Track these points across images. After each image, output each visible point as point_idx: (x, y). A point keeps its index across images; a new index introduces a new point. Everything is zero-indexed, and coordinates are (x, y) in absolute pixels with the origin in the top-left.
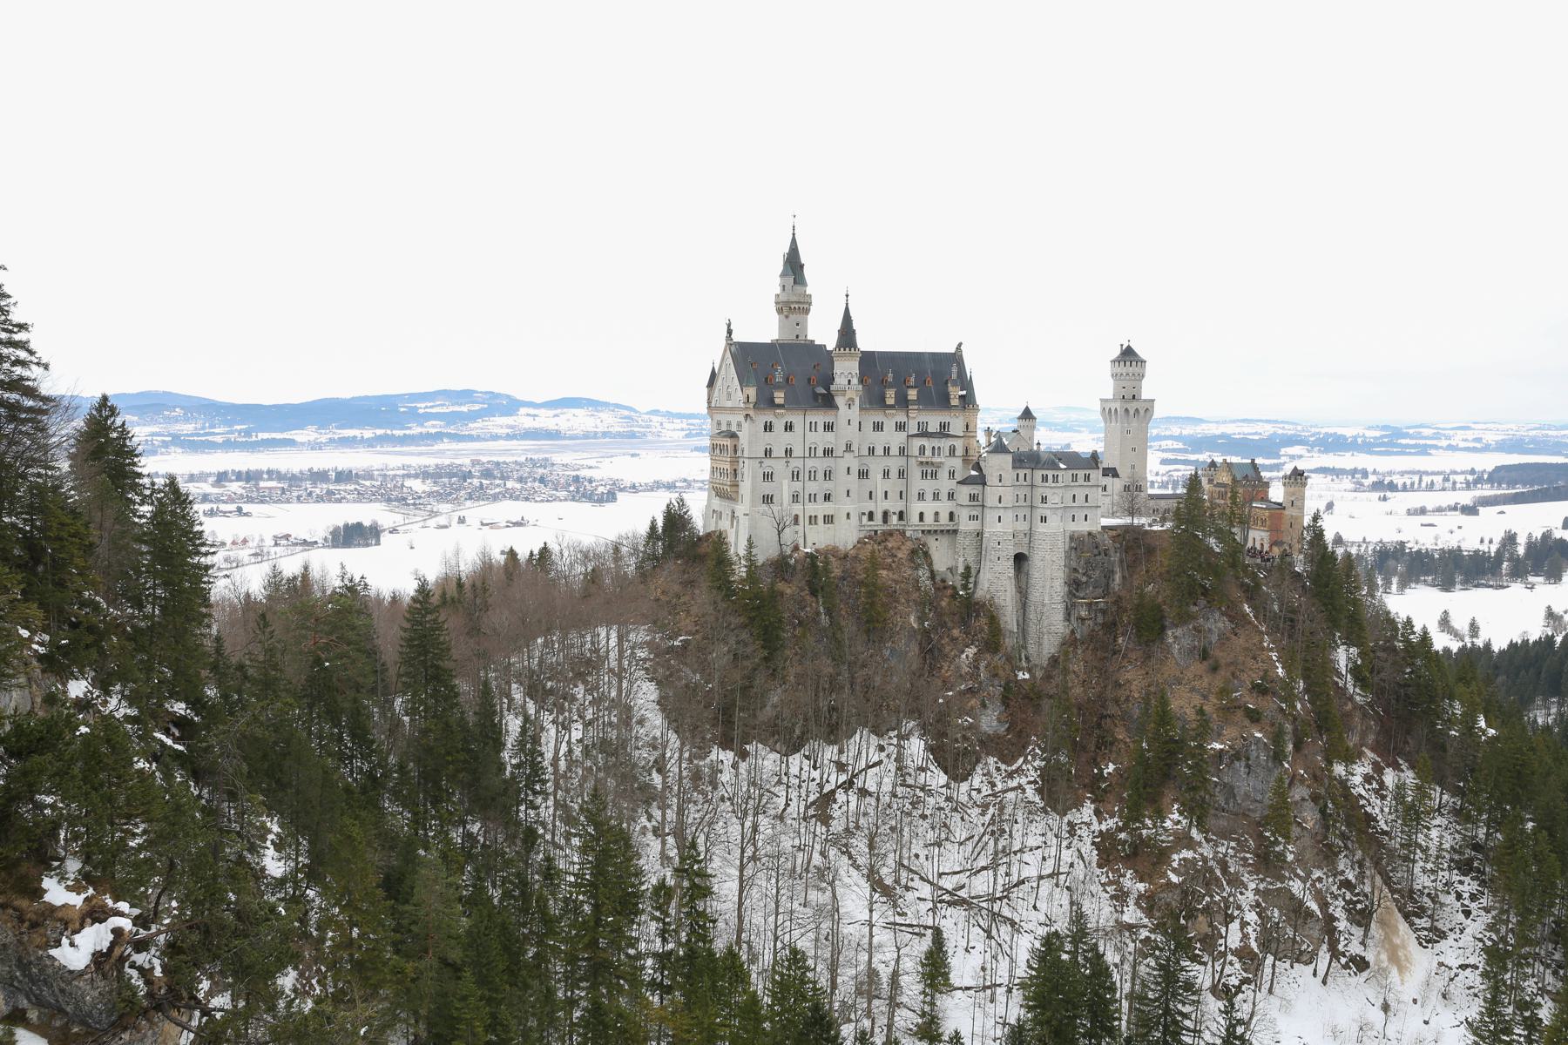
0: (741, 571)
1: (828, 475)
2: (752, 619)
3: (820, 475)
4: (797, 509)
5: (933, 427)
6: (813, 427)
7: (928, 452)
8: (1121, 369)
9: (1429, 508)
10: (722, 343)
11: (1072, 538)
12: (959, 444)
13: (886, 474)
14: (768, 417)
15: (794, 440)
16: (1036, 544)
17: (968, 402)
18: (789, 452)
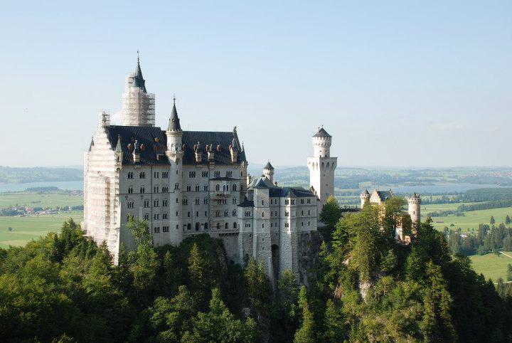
0: (116, 262)
1: (165, 203)
2: (126, 292)
3: (160, 204)
4: (148, 222)
5: (223, 175)
6: (156, 175)
7: (221, 189)
8: (320, 141)
9: (438, 212)
10: (101, 123)
11: (302, 235)
12: (238, 184)
13: (197, 202)
14: (130, 170)
15: (145, 183)
16: (283, 240)
17: (241, 157)
18: (142, 190)
